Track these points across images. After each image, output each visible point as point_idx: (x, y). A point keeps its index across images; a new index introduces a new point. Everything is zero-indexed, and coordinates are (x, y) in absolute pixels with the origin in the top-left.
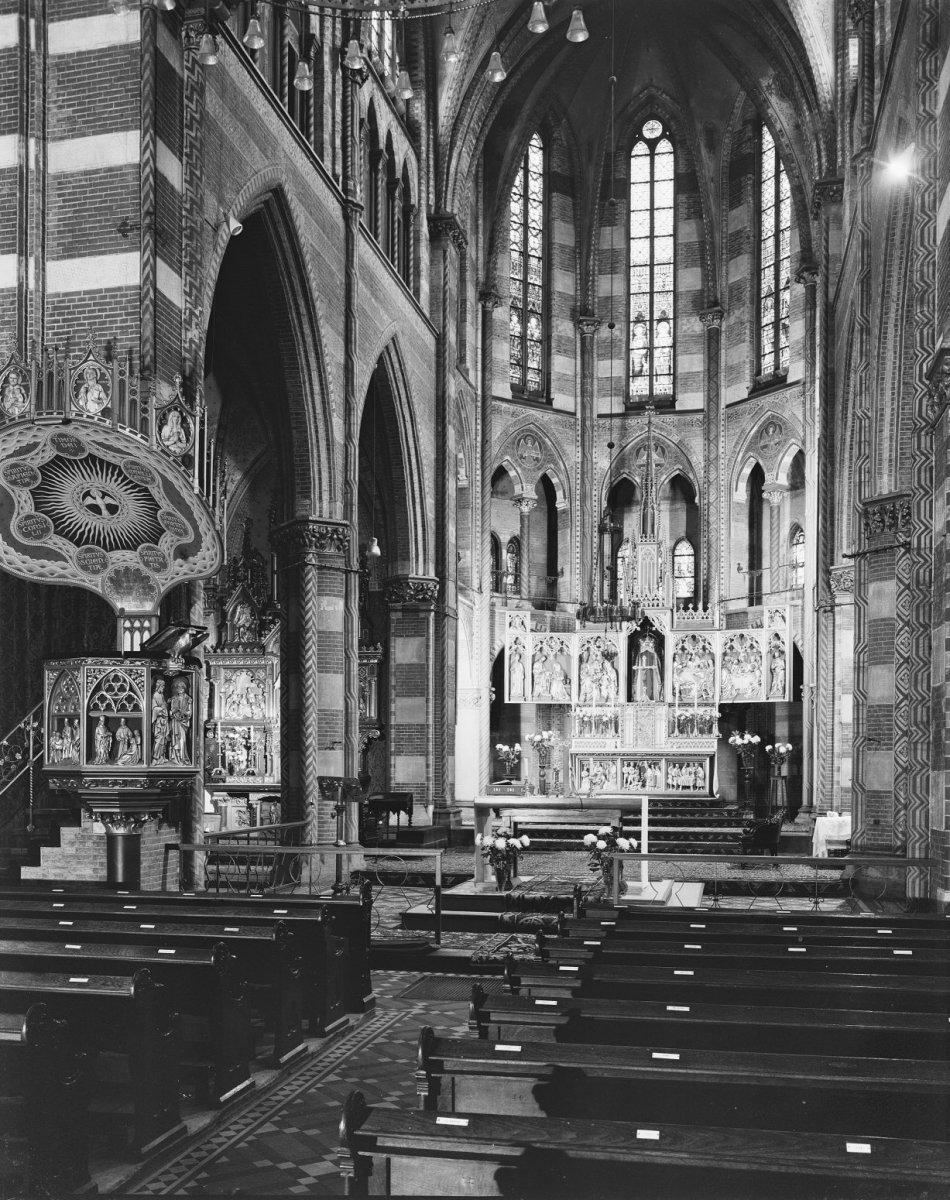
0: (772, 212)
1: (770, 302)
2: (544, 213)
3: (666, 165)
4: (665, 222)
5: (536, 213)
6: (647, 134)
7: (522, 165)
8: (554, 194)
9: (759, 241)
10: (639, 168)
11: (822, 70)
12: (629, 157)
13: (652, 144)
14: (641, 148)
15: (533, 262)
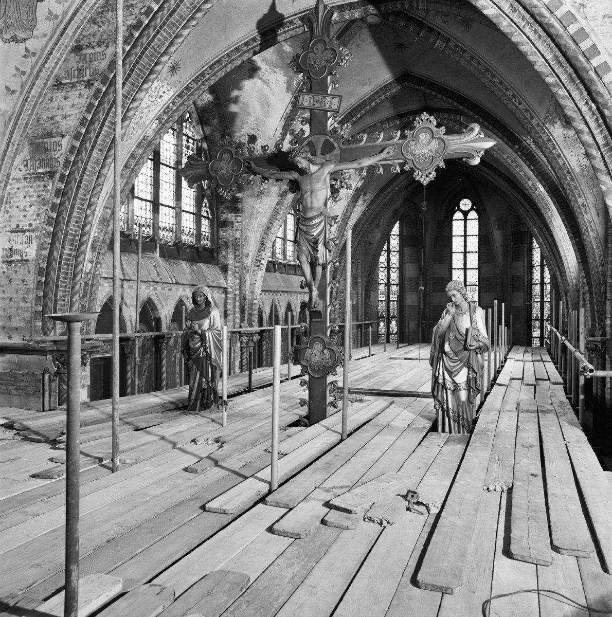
0: (538, 268)
1: (538, 324)
2: (400, 258)
3: (474, 226)
4: (473, 260)
5: (395, 259)
6: (462, 207)
7: (385, 247)
8: (406, 248)
9: (531, 284)
10: (457, 227)
11: (569, 258)
12: (452, 220)
13: (465, 213)
14: (458, 215)
15: (394, 289)
